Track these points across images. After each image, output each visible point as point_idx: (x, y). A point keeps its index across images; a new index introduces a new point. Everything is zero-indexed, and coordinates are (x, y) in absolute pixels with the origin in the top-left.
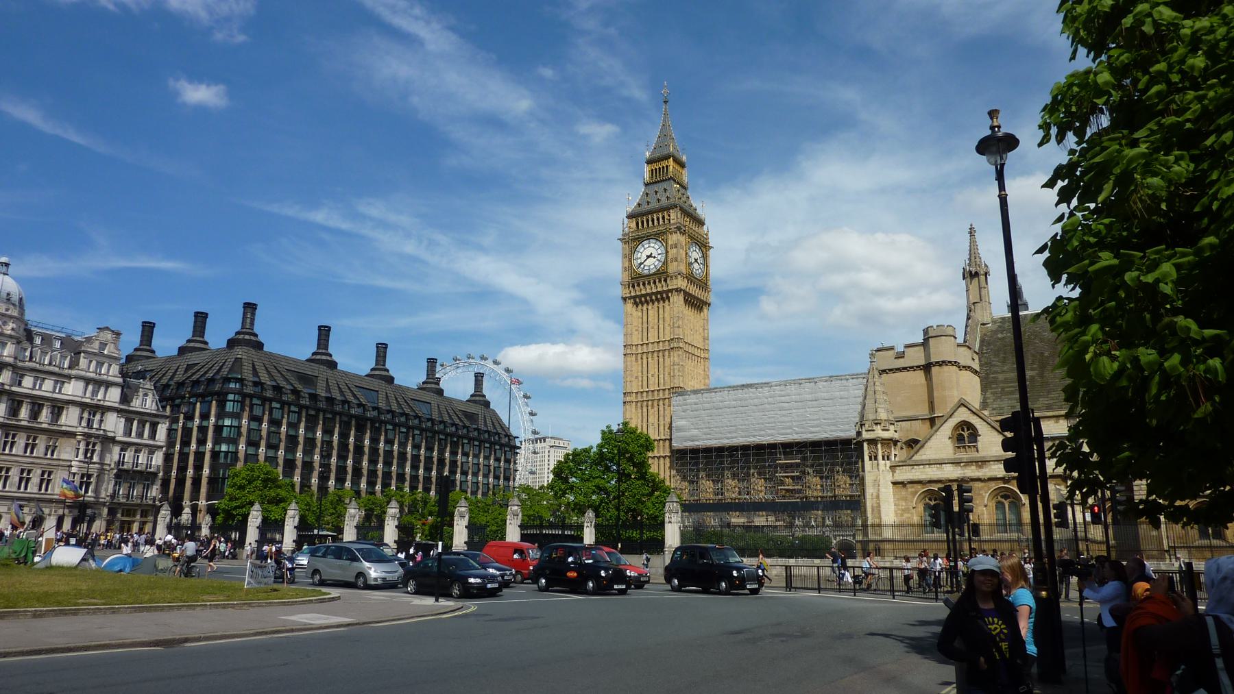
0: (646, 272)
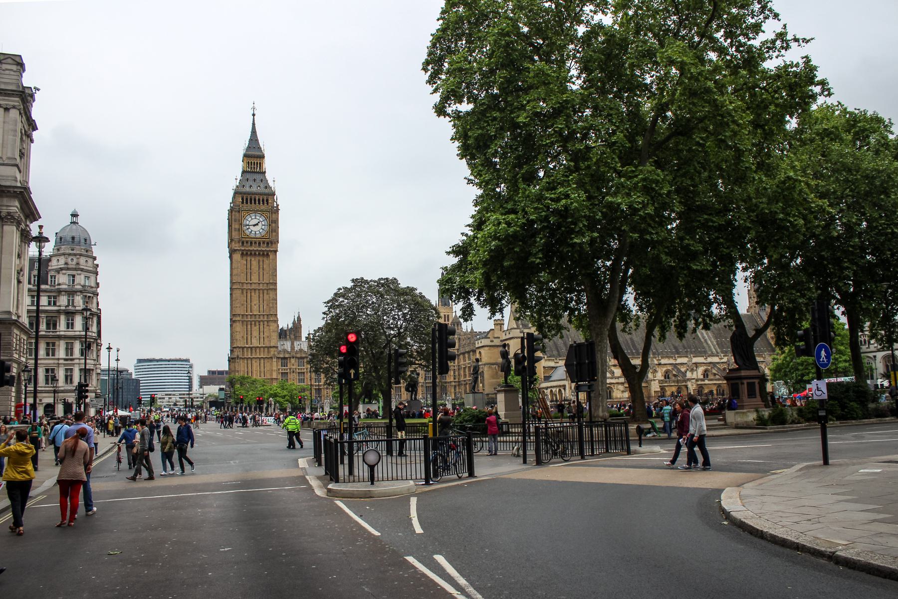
0: (253, 235)
